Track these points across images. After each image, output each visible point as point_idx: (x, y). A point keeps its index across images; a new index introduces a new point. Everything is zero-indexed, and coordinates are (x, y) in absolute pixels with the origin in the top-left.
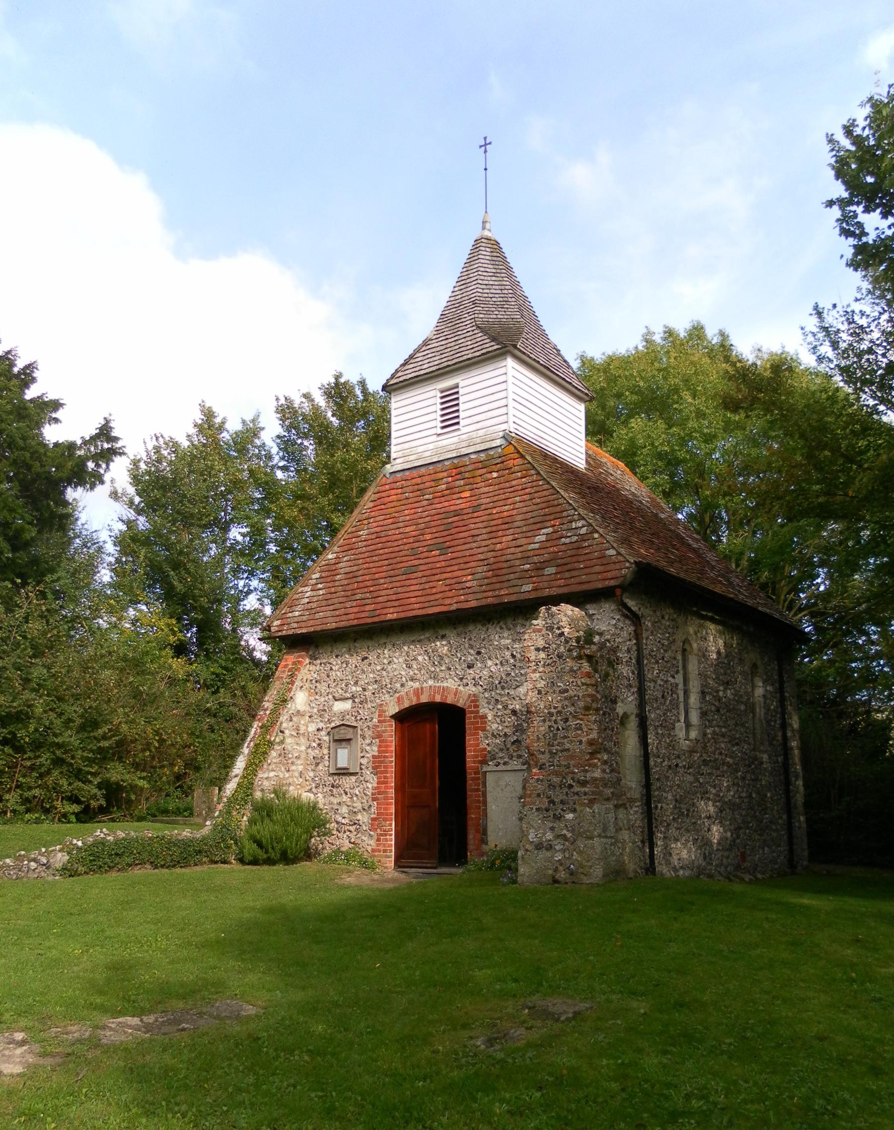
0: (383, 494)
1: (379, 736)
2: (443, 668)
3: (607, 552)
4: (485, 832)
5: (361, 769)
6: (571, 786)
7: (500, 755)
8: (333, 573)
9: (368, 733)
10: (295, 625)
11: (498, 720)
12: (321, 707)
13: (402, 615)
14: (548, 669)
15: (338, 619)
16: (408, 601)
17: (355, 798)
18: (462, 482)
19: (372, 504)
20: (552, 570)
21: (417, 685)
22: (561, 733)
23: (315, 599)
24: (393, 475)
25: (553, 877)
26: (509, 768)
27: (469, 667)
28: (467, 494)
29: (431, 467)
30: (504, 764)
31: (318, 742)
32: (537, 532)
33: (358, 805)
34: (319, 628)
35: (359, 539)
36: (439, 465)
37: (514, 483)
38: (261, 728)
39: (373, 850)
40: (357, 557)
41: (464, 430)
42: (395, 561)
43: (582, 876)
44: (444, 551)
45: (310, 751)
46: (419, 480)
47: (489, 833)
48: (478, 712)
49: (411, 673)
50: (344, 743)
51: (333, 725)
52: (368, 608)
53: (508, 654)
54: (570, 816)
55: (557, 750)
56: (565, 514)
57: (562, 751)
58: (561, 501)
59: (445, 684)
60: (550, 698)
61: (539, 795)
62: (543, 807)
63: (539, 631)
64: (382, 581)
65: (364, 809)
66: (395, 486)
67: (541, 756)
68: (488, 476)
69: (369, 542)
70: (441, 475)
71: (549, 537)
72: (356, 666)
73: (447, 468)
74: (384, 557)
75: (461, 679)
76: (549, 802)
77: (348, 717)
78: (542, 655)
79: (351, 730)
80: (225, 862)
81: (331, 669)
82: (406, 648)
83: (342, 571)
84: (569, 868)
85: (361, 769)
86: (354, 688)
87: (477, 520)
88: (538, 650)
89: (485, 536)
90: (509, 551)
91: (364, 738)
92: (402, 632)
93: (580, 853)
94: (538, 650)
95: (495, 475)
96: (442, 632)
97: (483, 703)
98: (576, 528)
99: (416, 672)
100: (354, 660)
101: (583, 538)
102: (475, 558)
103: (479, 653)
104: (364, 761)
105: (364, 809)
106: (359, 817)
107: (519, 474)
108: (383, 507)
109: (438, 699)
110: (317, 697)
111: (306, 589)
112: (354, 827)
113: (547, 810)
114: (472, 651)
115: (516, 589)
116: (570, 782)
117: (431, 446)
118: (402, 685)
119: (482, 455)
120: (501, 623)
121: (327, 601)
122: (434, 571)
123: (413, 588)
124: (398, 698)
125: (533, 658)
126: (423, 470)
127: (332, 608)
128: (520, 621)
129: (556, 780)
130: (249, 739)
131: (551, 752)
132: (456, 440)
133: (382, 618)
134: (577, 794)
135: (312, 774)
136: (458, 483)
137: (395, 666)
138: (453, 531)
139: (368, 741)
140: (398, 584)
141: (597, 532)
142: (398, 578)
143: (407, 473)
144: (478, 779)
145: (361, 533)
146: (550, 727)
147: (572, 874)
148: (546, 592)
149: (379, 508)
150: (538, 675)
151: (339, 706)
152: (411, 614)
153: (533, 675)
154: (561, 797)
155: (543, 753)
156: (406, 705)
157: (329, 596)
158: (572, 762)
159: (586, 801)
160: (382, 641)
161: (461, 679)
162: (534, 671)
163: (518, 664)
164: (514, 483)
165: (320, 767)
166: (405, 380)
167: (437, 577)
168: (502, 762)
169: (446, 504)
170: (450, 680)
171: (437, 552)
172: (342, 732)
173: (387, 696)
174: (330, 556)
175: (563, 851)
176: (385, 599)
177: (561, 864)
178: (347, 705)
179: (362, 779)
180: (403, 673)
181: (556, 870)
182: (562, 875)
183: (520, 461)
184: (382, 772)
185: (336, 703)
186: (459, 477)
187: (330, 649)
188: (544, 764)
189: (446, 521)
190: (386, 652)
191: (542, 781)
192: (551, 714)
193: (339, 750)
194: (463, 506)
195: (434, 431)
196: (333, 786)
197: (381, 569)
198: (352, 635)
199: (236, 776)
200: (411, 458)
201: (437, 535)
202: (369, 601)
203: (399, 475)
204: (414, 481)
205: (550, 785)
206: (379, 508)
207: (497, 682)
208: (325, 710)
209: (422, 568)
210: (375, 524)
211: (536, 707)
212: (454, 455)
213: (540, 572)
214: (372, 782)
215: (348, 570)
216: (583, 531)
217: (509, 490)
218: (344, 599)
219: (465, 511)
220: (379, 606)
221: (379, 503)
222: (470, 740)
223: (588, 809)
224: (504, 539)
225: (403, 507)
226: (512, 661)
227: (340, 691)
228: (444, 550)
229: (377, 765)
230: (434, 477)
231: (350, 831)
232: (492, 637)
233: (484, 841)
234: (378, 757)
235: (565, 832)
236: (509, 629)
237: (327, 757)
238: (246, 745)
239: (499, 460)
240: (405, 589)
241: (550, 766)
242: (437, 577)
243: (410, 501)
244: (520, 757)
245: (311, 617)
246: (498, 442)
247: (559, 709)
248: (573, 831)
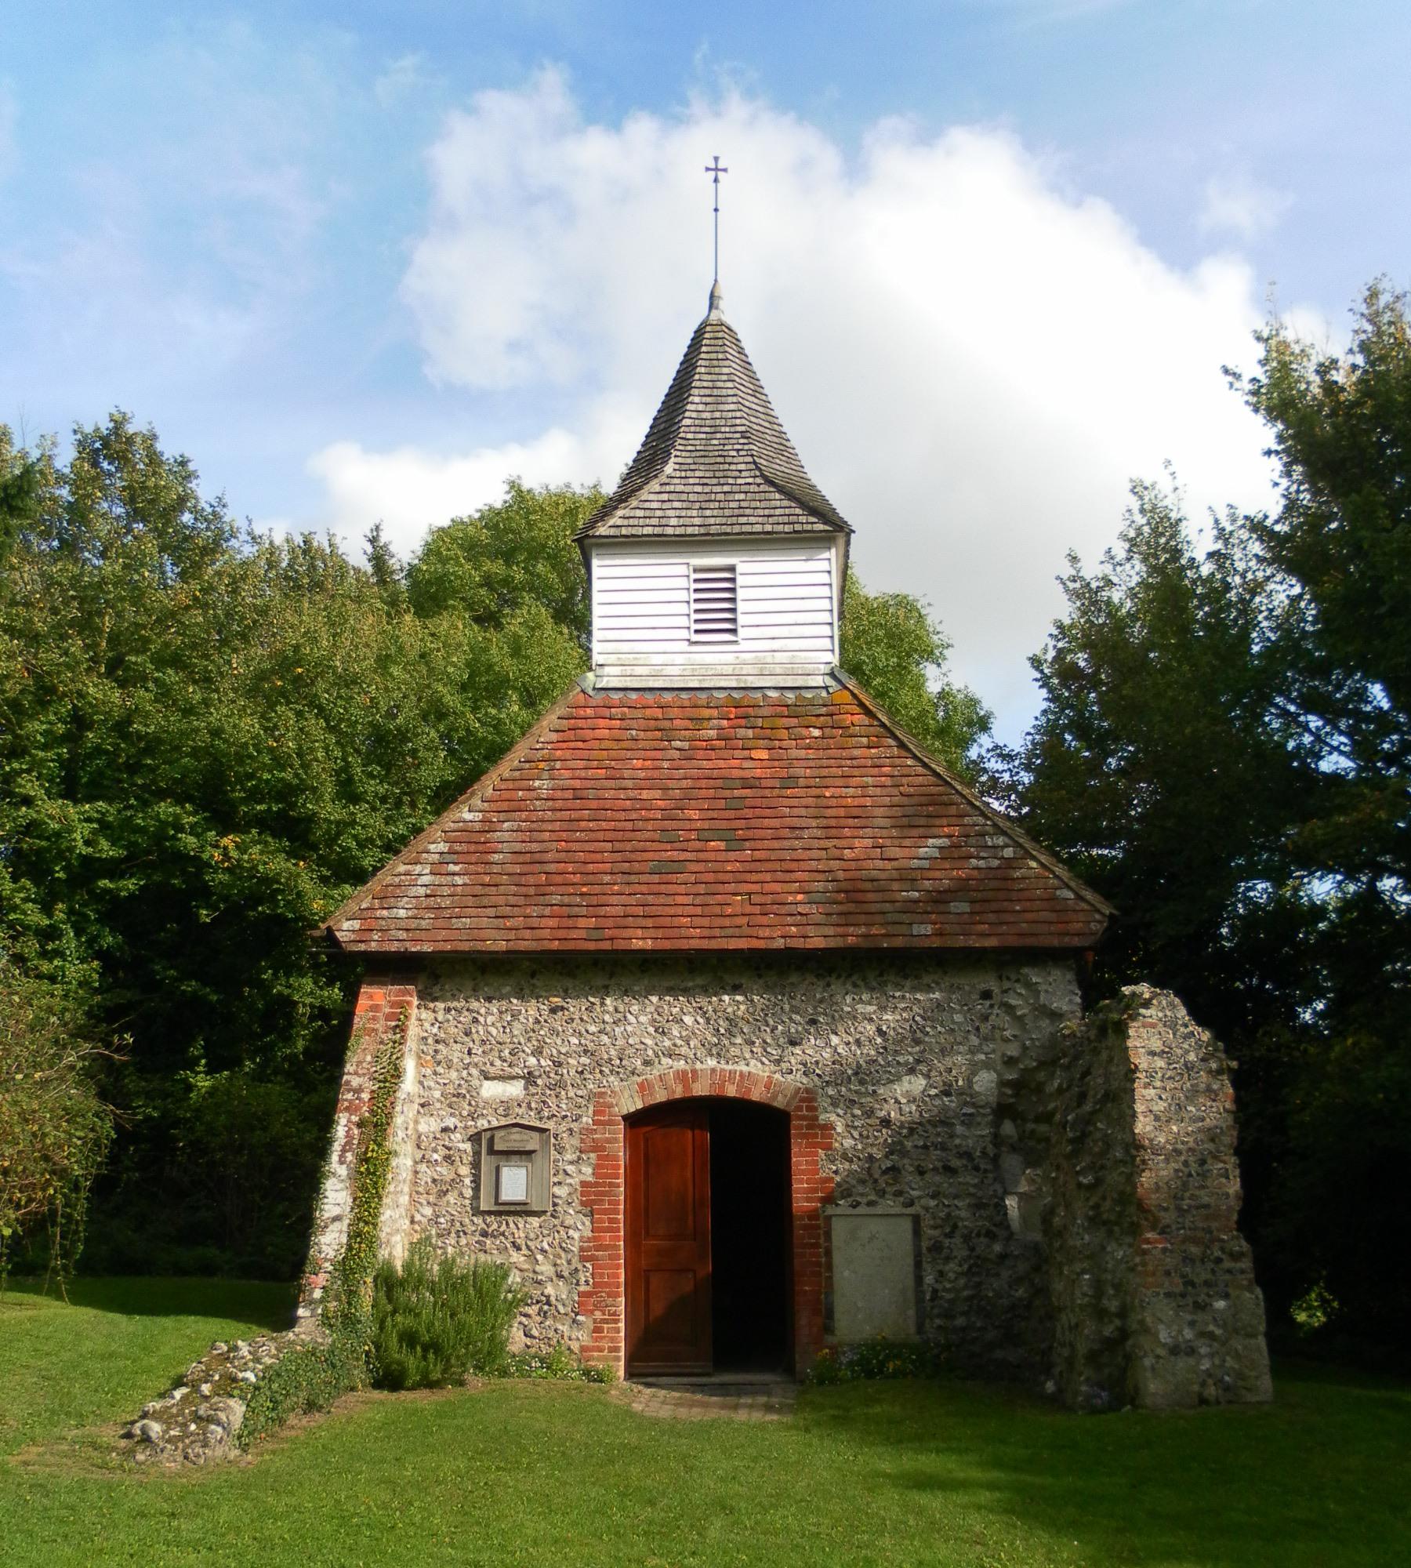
0: (580, 723)
1: (596, 1148)
2: (739, 1040)
3: (1058, 893)
4: (830, 1314)
5: (555, 1205)
6: (1219, 1261)
7: (861, 1189)
8: (481, 848)
9: (571, 1142)
10: (403, 935)
11: (856, 1134)
12: (451, 1089)
13: (667, 945)
14: (1170, 1085)
15: (512, 935)
16: (676, 921)
17: (540, 1257)
18: (750, 733)
19: (554, 737)
20: (965, 907)
21: (681, 1064)
22: (1194, 1182)
23: (446, 891)
24: (603, 694)
25: (1200, 1395)
26: (879, 1210)
27: (793, 1043)
28: (764, 755)
29: (684, 695)
30: (870, 1204)
31: (443, 1152)
32: (920, 842)
33: (546, 1269)
34: (465, 947)
35: (533, 794)
36: (703, 695)
37: (856, 752)
38: (360, 1125)
39: (583, 1349)
40: (534, 826)
41: (744, 646)
42: (628, 846)
43: (1244, 1392)
44: (734, 845)
45: (423, 1167)
46: (658, 713)
47: (837, 1315)
48: (816, 1118)
49: (667, 1043)
51: (482, 1124)
52: (582, 922)
53: (871, 1029)
54: (1221, 1304)
55: (1190, 1207)
56: (967, 820)
57: (1197, 1208)
58: (957, 798)
59: (745, 1069)
60: (1175, 1128)
61: (1168, 1273)
62: (1177, 1291)
63: (1153, 1026)
64: (607, 878)
65: (560, 1276)
66: (606, 712)
67: (1162, 1214)
68: (804, 732)
69: (559, 804)
70: (707, 713)
71: (946, 854)
72: (537, 1022)
73: (721, 703)
74: (601, 835)
75: (778, 1062)
76: (1186, 1284)
77: (517, 1110)
78: (1160, 1063)
79: (536, 1135)
80: (353, 1389)
81: (475, 1021)
82: (654, 999)
83: (505, 847)
84: (1221, 1381)
85: (555, 1205)
86: (532, 1061)
87: (794, 802)
88: (1153, 1053)
89: (819, 833)
90: (870, 864)
91: (560, 1150)
92: (643, 972)
93: (1237, 1356)
94: (1153, 1053)
95: (816, 733)
96: (731, 980)
97: (824, 1103)
98: (993, 847)
99: (679, 1042)
100: (531, 1010)
101: (1009, 864)
102: (804, 865)
103: (813, 1022)
104: (562, 1191)
105: (560, 1276)
106: (550, 1290)
107: (865, 740)
108: (580, 745)
109: (731, 1091)
110: (440, 1069)
111: (418, 868)
112: (536, 1308)
113: (1183, 1295)
114: (797, 1018)
115: (904, 929)
116: (1218, 1253)
117: (680, 659)
118: (646, 1063)
119: (790, 695)
120: (854, 978)
121: (477, 898)
122: (721, 877)
123: (680, 899)
124: (641, 1086)
125: (1143, 1066)
126: (668, 697)
127: (491, 912)
128: (892, 978)
129: (1194, 1250)
130: (337, 1147)
131: (1179, 1209)
132: (730, 658)
133: (621, 945)
134: (1229, 1271)
135: (428, 1211)
136: (741, 732)
137: (629, 1028)
138: (749, 813)
139: (569, 1156)
140: (644, 888)
141: (1034, 858)
142: (644, 878)
143: (634, 696)
144: (818, 1227)
145: (537, 783)
146: (1176, 1171)
147: (1227, 1388)
148: (961, 942)
149: (572, 745)
150: (1152, 1092)
151: (491, 1090)
152: (684, 945)
153: (1145, 1092)
154: (1205, 1276)
155: (1166, 1209)
156: (660, 1096)
157: (478, 890)
158: (1214, 1225)
159: (1245, 1283)
160: (599, 982)
161: (778, 1062)
162: (1147, 1086)
163: (891, 1047)
164: (856, 752)
165: (451, 1197)
166: (633, 536)
167: (731, 887)
168: (864, 1200)
169: (721, 764)
170: (753, 1062)
171: (722, 845)
172: (513, 1137)
173: (611, 1079)
174: (468, 816)
175: (1211, 1356)
176: (620, 911)
177: (1210, 1376)
178: (515, 1089)
179: (556, 1222)
180: (649, 1042)
181: (1203, 1384)
182: (1211, 1391)
183: (862, 719)
184: (605, 1212)
185: (487, 1083)
186: (743, 722)
187: (470, 984)
188: (1168, 1226)
189: (727, 794)
190: (608, 1001)
191: (1171, 1251)
192: (1178, 1152)
193: (506, 1172)
194: (758, 773)
195: (684, 634)
196: (484, 1234)
197: (598, 857)
199: (337, 1218)
200: (639, 670)
201: (715, 814)
202: (584, 911)
203: (616, 696)
204: (648, 712)
205: (1184, 1259)
206: (572, 745)
207: (850, 1072)
208: (458, 1095)
209: (694, 867)
210: (567, 774)
211: (1151, 1140)
212: (734, 685)
213: (942, 908)
214: (580, 1228)
215: (518, 847)
216: (1008, 852)
217: (849, 762)
218: (521, 901)
219: (764, 783)
220: (610, 922)
221: (572, 733)
222: (799, 1160)
223: (1248, 1295)
224: (857, 843)
225: (629, 754)
226: (879, 1040)
227: (498, 1063)
228: (735, 843)
229: (591, 1199)
230: (690, 712)
231: (526, 1315)
232: (839, 998)
233: (828, 1329)
234: (596, 1185)
235: (1211, 1328)
236: (873, 989)
237: (467, 1181)
238: (335, 1157)
239: (824, 710)
240: (662, 900)
241: (1179, 1229)
242: (731, 887)
243: (641, 745)
244: (899, 1193)
245: (440, 923)
246: (818, 681)
247: (1191, 1145)
248: (1224, 1326)
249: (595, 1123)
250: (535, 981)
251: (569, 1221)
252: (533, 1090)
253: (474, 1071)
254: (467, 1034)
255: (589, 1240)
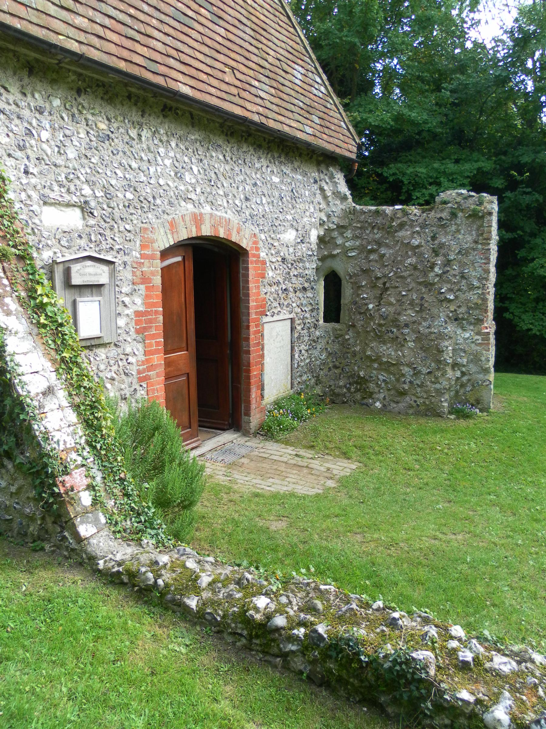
50: (94, 290)
77: (78, 241)
79: (105, 268)
139: (125, 289)
168: (276, 311)
185: (47, 209)
198: (73, 77)
199: (49, 391)
249: (143, 256)
250: (80, 100)
251: (128, 350)
252: (92, 222)
253: (35, 195)
254: (21, 148)
255: (143, 363)
